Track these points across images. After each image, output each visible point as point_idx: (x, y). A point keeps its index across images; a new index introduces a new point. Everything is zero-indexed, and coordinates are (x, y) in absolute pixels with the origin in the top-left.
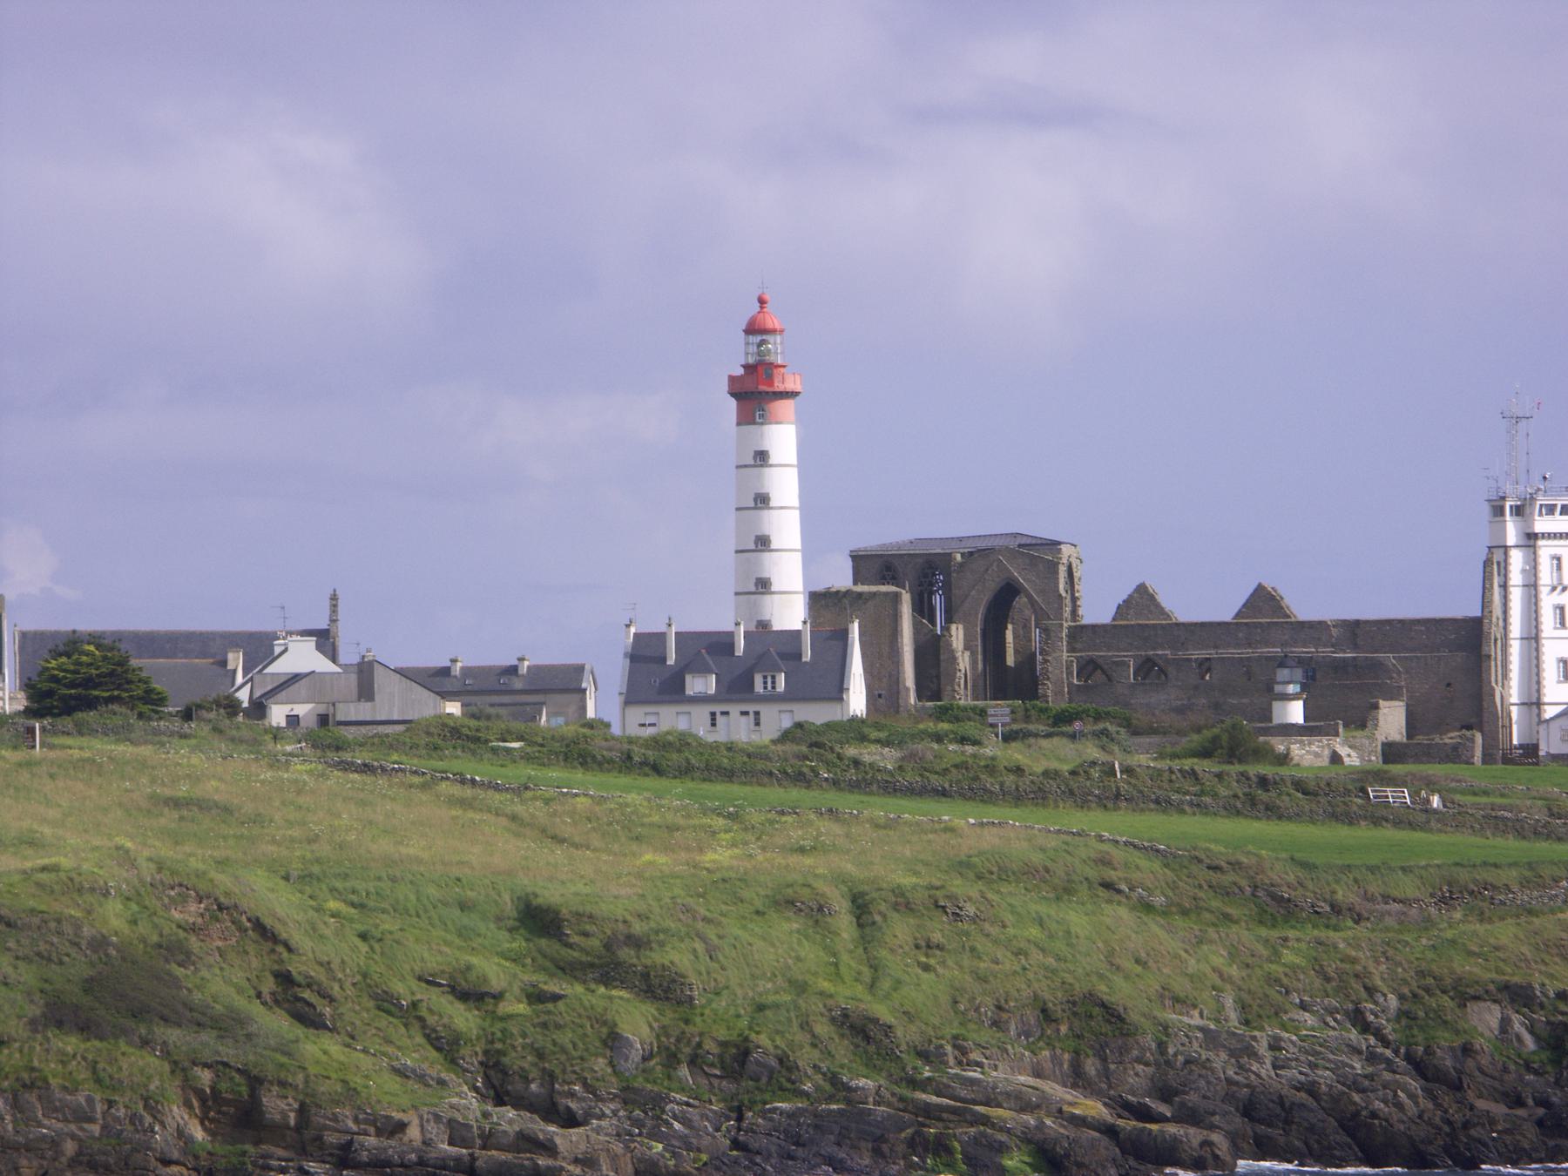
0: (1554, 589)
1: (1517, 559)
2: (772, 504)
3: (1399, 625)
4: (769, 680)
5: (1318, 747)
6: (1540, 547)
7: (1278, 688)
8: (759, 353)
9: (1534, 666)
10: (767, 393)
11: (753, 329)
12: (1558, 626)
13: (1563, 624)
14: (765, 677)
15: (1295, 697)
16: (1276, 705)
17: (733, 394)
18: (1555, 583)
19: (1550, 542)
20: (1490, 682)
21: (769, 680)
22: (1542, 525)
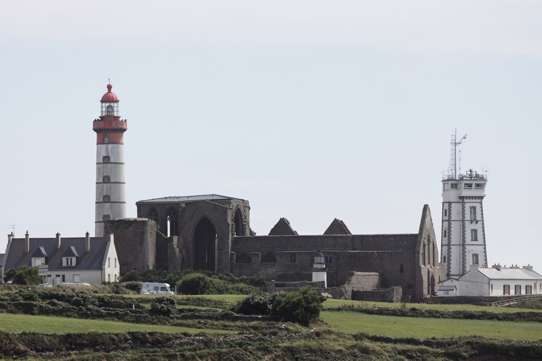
0: (472, 222)
1: (456, 208)
2: (112, 180)
4: (69, 261)
7: (315, 266)
8: (108, 112)
9: (461, 258)
10: (109, 129)
13: (476, 239)
14: (67, 259)
15: (323, 270)
16: (314, 274)
17: (95, 130)
18: (473, 219)
19: (471, 200)
20: (419, 264)
21: (69, 261)
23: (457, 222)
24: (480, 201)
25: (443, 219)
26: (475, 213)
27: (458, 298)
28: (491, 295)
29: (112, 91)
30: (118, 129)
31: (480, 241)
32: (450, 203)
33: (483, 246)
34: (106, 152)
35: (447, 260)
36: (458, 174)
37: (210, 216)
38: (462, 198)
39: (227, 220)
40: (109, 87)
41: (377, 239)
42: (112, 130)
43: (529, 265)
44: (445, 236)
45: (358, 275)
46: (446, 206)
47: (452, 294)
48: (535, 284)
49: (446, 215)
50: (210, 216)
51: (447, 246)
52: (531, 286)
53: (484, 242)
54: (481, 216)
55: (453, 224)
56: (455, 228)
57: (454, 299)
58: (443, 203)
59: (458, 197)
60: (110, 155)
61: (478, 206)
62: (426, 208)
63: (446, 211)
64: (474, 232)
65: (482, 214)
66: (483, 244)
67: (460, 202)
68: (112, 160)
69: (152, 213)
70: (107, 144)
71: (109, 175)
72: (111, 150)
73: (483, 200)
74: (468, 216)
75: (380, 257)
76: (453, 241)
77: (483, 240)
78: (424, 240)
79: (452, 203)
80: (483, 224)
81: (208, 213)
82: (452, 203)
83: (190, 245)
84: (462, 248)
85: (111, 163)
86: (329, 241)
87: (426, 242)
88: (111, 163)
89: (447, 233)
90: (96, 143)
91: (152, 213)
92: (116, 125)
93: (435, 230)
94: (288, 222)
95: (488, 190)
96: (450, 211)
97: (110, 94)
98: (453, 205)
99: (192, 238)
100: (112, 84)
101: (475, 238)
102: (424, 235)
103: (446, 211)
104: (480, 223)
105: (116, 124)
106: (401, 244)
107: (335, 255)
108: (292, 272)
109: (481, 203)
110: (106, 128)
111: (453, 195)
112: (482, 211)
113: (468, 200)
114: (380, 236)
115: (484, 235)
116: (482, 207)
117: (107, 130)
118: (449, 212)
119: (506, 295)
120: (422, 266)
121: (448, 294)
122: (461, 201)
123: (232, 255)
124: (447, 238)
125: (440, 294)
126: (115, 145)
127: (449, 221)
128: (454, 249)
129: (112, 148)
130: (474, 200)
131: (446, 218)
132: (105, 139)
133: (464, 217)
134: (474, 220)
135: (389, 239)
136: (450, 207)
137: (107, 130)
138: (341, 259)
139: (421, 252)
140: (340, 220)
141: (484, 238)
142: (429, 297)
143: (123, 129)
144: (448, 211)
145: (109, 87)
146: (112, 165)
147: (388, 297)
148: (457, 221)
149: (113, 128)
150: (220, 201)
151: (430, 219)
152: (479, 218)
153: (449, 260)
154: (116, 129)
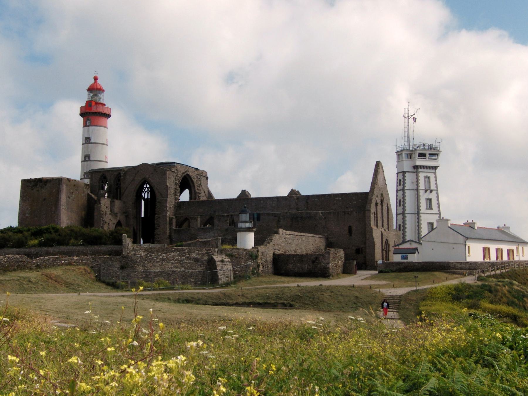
0: (426, 191)
1: (409, 178)
2: (91, 159)
3: (329, 197)
5: (198, 254)
6: (419, 172)
7: (240, 225)
9: (417, 226)
10: (90, 113)
11: (91, 89)
12: (428, 208)
13: (431, 208)
15: (249, 230)
16: (239, 235)
17: (80, 115)
18: (427, 188)
19: (425, 170)
20: (370, 225)
22: (420, 162)
23: (411, 191)
24: (434, 171)
25: (397, 189)
26: (429, 182)
27: (422, 264)
28: (469, 259)
29: (97, 82)
30: (99, 113)
31: (435, 210)
32: (404, 173)
33: (438, 215)
35: (402, 228)
36: (411, 144)
37: (150, 179)
38: (416, 167)
39: (166, 182)
40: (96, 79)
41: (323, 199)
42: (93, 113)
43: (505, 225)
44: (400, 205)
45: (286, 234)
46: (401, 176)
47: (413, 258)
48: (517, 247)
49: (400, 184)
51: (401, 215)
52: (513, 251)
53: (439, 210)
54: (435, 185)
55: (408, 193)
56: (409, 196)
57: (416, 266)
58: (397, 173)
59: (412, 168)
60: (91, 136)
61: (432, 176)
62: (378, 165)
63: (400, 181)
64: (429, 200)
65: (436, 184)
66: (438, 213)
67: (414, 172)
68: (92, 141)
69: (103, 181)
70: (88, 126)
71: (90, 153)
73: (437, 170)
74: (422, 186)
75: (325, 218)
76: (408, 210)
77: (438, 209)
78: (376, 199)
79: (406, 173)
80: (437, 194)
82: (406, 173)
83: (130, 210)
84: (417, 217)
85: (92, 143)
86: (272, 202)
87: (379, 201)
88: (92, 143)
89: (401, 203)
90: (82, 126)
91: (103, 180)
92: (96, 109)
93: (389, 192)
94: (249, 194)
95: (441, 162)
96: (404, 180)
98: (407, 174)
99: (133, 203)
100: (98, 75)
101: (430, 206)
102: (375, 193)
103: (400, 181)
104: (434, 193)
106: (350, 203)
107: (275, 216)
108: (230, 237)
109: (435, 173)
110: (86, 112)
111: (407, 165)
112: (436, 180)
113: (422, 170)
114: (327, 196)
115: (438, 204)
116: (436, 177)
117: (88, 113)
118: (403, 182)
119: (487, 260)
120: (374, 227)
121: (407, 258)
122: (415, 170)
123: (171, 219)
124: (402, 207)
125: (397, 258)
127: (403, 190)
128: (408, 218)
130: (428, 170)
131: (401, 187)
133: (418, 185)
134: (428, 190)
135: (336, 199)
136: (404, 176)
137: (88, 113)
138: (282, 221)
139: (373, 210)
140: (297, 190)
141: (439, 207)
142: (381, 263)
144: (402, 180)
145: (96, 79)
146: (92, 144)
147: (322, 262)
148: (412, 190)
149: (93, 111)
150: (164, 165)
151: (383, 178)
152: (433, 187)
153: (404, 228)
154: (96, 113)
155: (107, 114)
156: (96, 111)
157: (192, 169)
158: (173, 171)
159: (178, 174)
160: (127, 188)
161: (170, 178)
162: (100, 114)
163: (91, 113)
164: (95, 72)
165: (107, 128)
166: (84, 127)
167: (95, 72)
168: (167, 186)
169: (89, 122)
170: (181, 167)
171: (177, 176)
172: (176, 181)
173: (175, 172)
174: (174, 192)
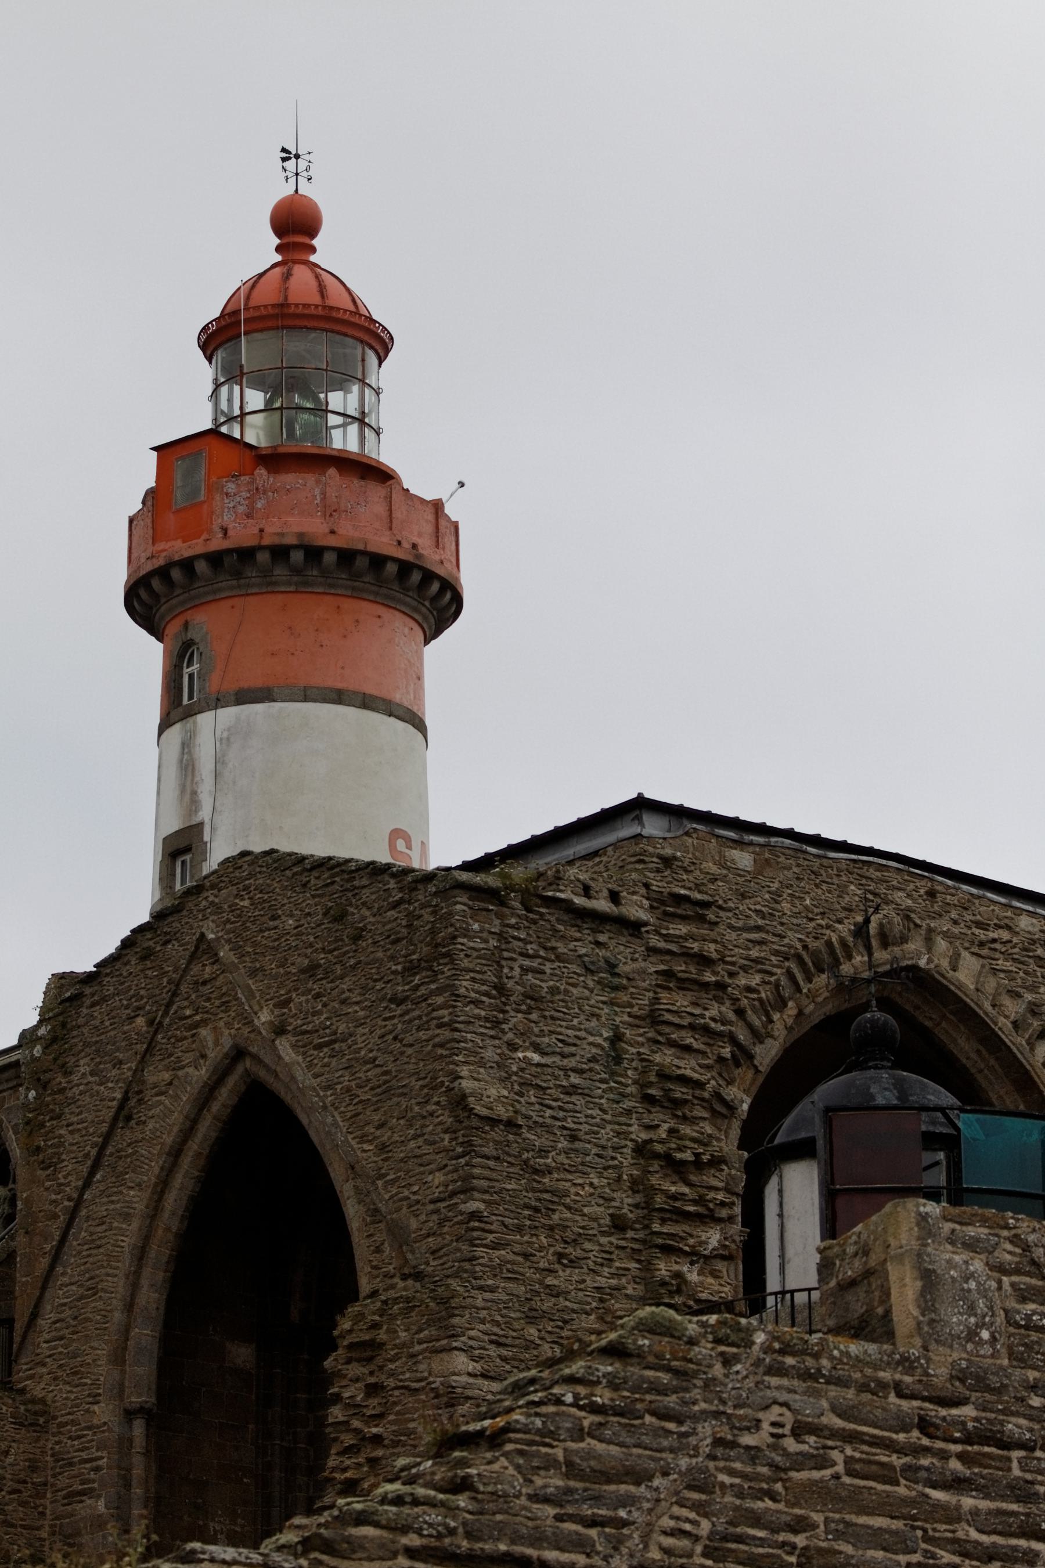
10: (187, 565)
29: (313, 258)
30: (280, 552)
34: (183, 790)
42: (215, 559)
50: (284, 1047)
70: (190, 713)
72: (219, 761)
81: (265, 1016)
97: (300, 271)
99: (129, 1415)
105: (251, 507)
110: (160, 562)
117: (176, 574)
126: (259, 707)
129: (224, 742)
132: (186, 671)
143: (332, 541)
149: (217, 543)
154: (246, 554)
155: (378, 561)
156: (243, 535)
157: (982, 911)
158: (602, 904)
159: (704, 961)
160: (73, 1215)
161: (532, 997)
162: (297, 557)
163: (201, 567)
164: (287, 154)
165: (420, 726)
166: (162, 729)
167: (287, 154)
168: (460, 1102)
169: (195, 667)
170: (762, 865)
171: (684, 984)
172: (665, 1057)
173: (634, 927)
174: (625, 1201)
